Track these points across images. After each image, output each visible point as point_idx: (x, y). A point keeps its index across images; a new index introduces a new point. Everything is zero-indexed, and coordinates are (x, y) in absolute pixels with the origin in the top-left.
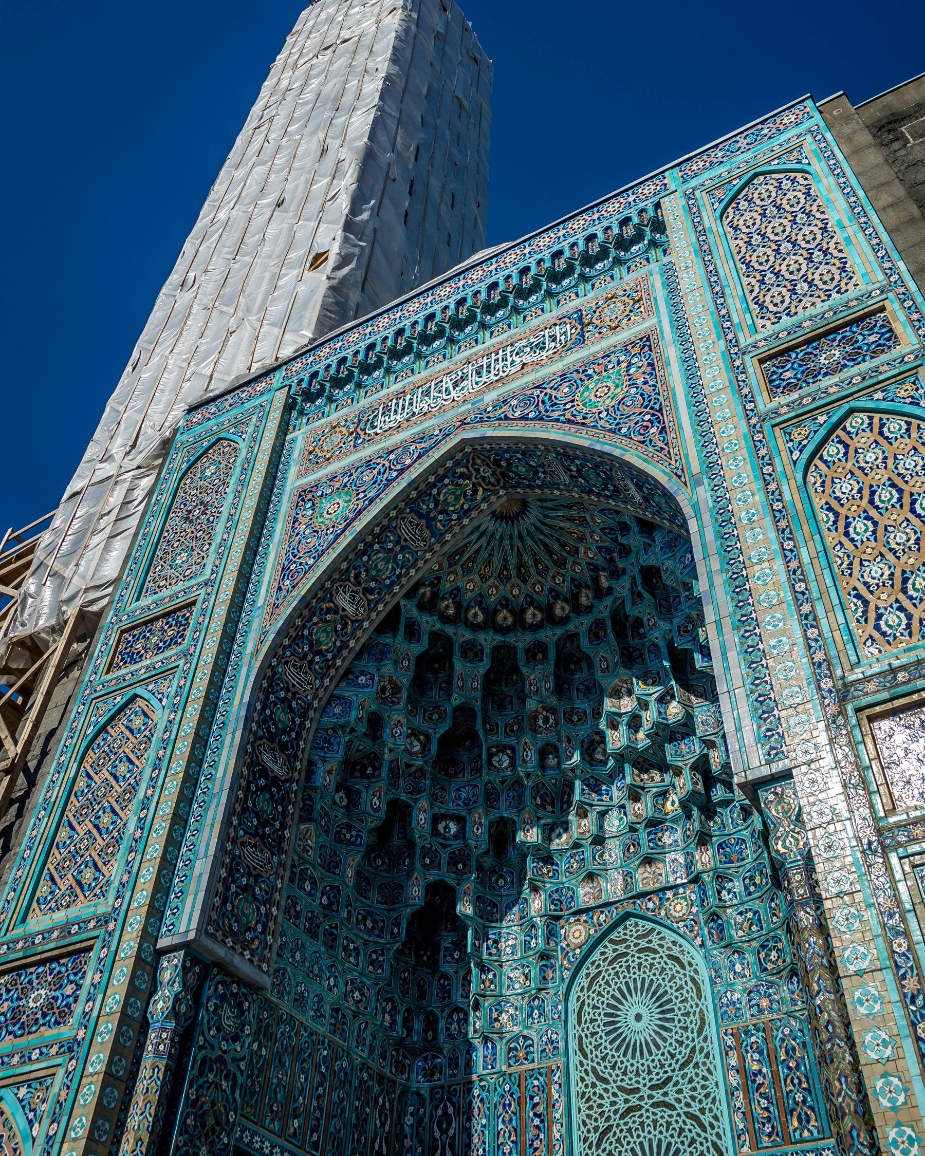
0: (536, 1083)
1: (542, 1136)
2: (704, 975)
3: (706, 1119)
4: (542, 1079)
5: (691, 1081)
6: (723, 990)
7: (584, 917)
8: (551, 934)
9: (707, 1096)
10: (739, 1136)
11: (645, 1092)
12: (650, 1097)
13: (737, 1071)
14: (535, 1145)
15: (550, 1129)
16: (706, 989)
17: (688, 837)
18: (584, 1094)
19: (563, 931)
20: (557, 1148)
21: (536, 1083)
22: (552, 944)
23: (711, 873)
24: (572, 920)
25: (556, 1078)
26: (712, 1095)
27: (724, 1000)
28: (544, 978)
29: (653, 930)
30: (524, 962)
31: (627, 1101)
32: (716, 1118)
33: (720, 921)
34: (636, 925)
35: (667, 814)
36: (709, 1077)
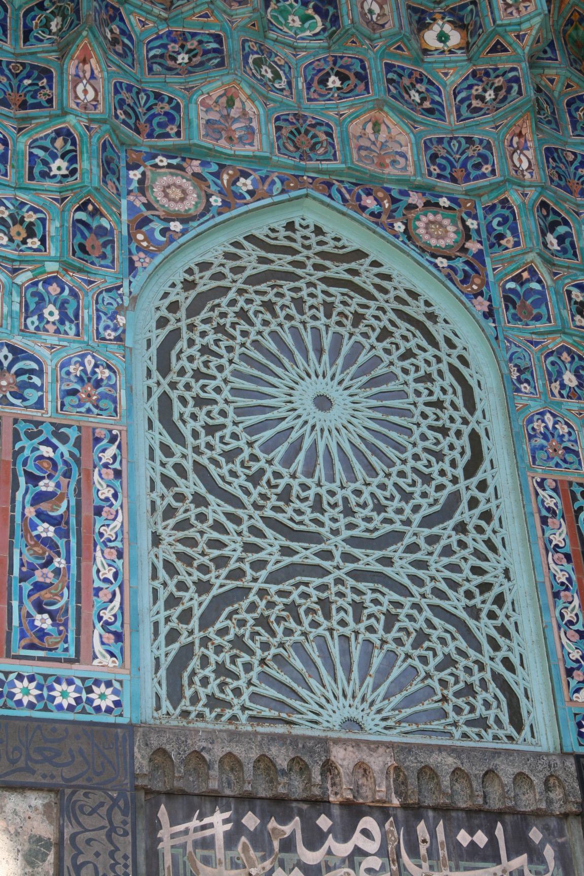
0: (46, 451)
1: (59, 562)
2: (485, 371)
3: (483, 628)
4: (63, 449)
5: (447, 551)
6: (535, 406)
7: (195, 166)
8: (109, 168)
9: (485, 587)
10: (569, 672)
11: (337, 545)
12: (348, 557)
13: (568, 557)
14: (38, 576)
15: (84, 553)
16: (490, 397)
17: (477, 110)
18: (170, 512)
19: (135, 175)
20: (104, 596)
21: (46, 451)
22: (110, 190)
23: (532, 193)
24: (162, 161)
25: (107, 457)
26: (496, 590)
27: (539, 426)
28: (82, 247)
29: (359, 254)
30: (23, 196)
31: (286, 551)
32: (503, 631)
33: (535, 286)
34: (318, 231)
35: (426, 51)
36: (490, 554)
